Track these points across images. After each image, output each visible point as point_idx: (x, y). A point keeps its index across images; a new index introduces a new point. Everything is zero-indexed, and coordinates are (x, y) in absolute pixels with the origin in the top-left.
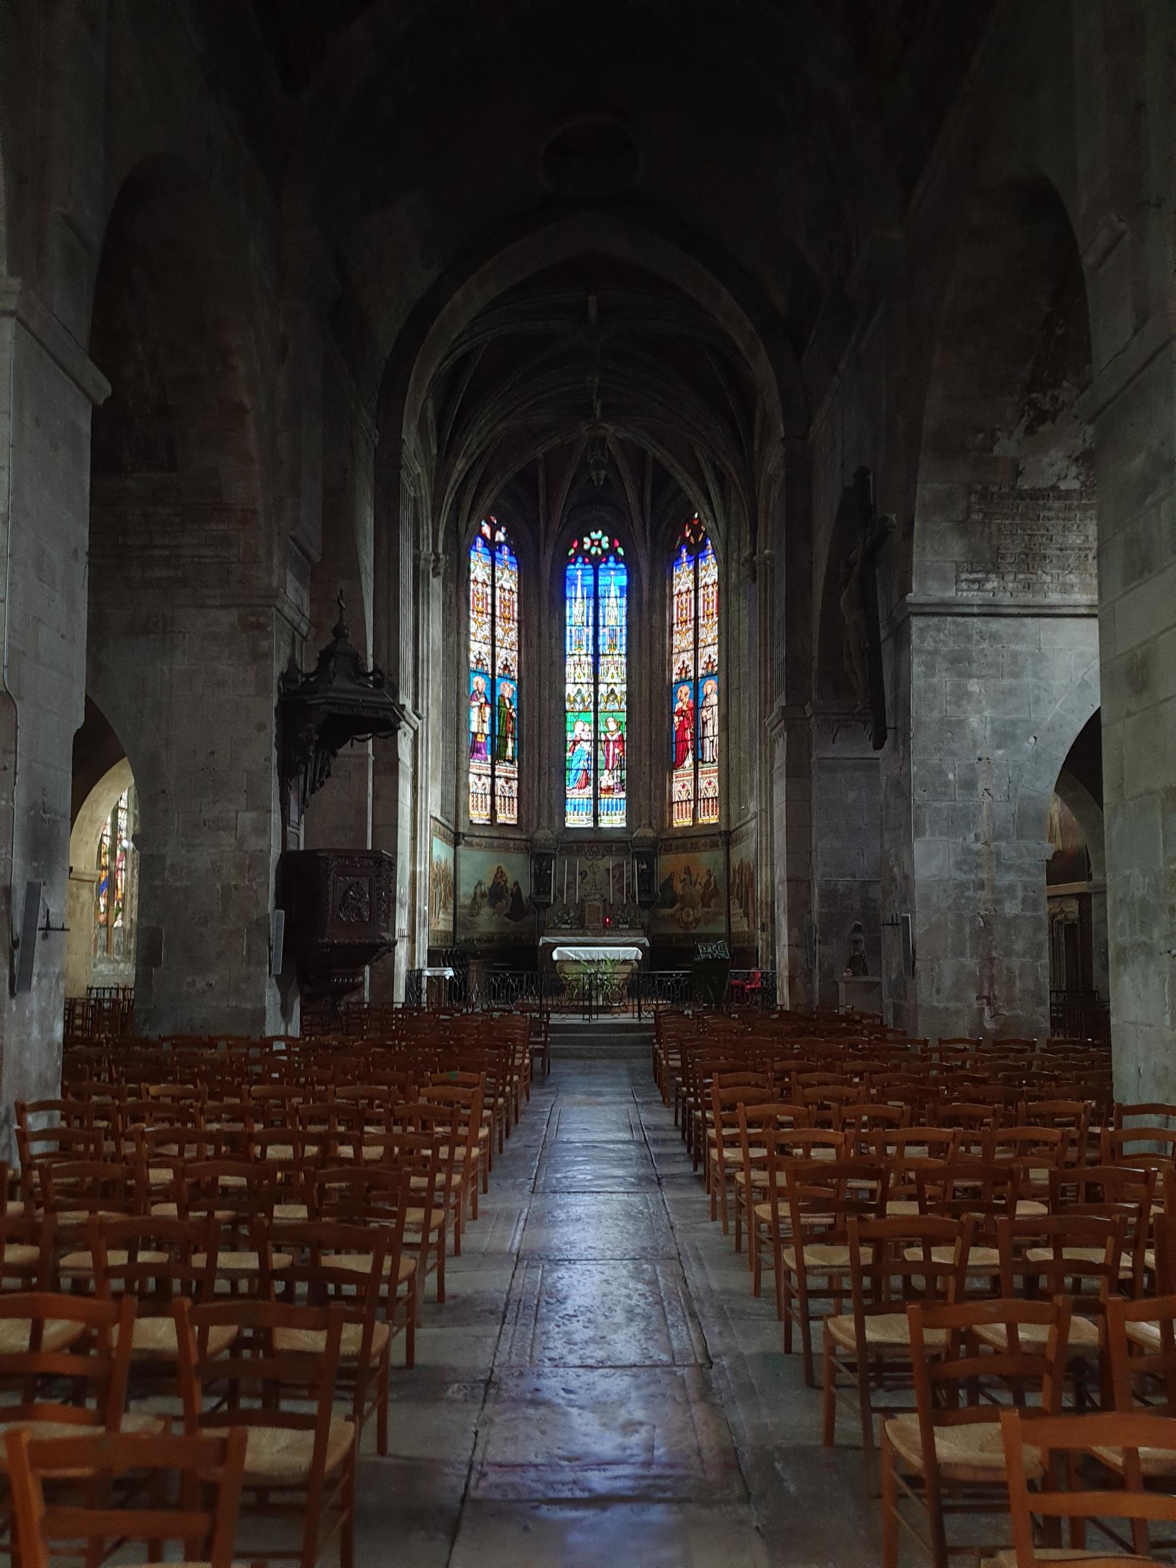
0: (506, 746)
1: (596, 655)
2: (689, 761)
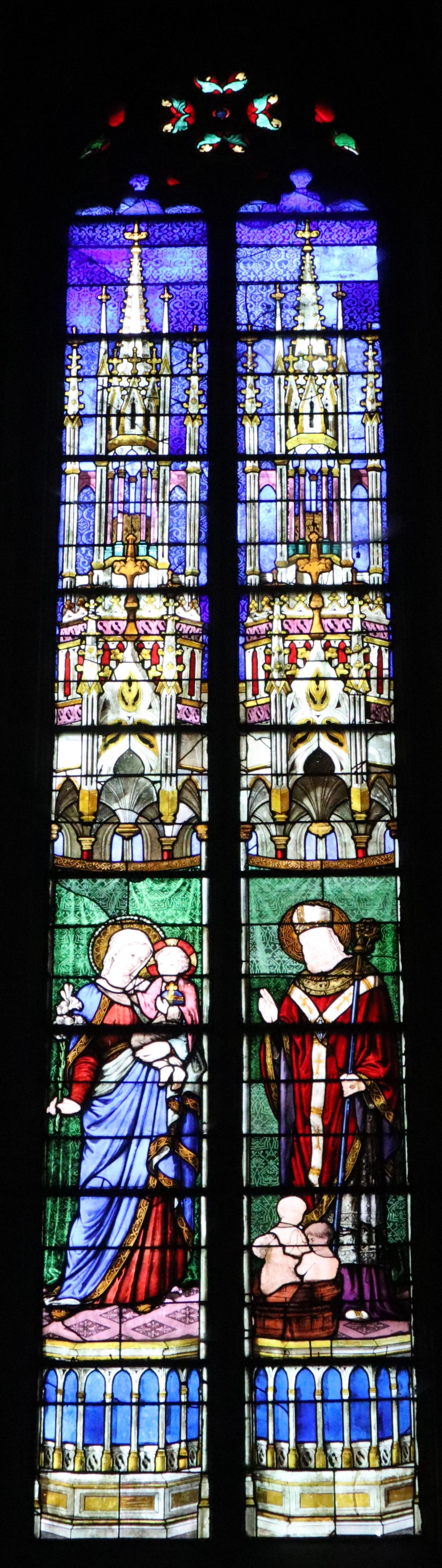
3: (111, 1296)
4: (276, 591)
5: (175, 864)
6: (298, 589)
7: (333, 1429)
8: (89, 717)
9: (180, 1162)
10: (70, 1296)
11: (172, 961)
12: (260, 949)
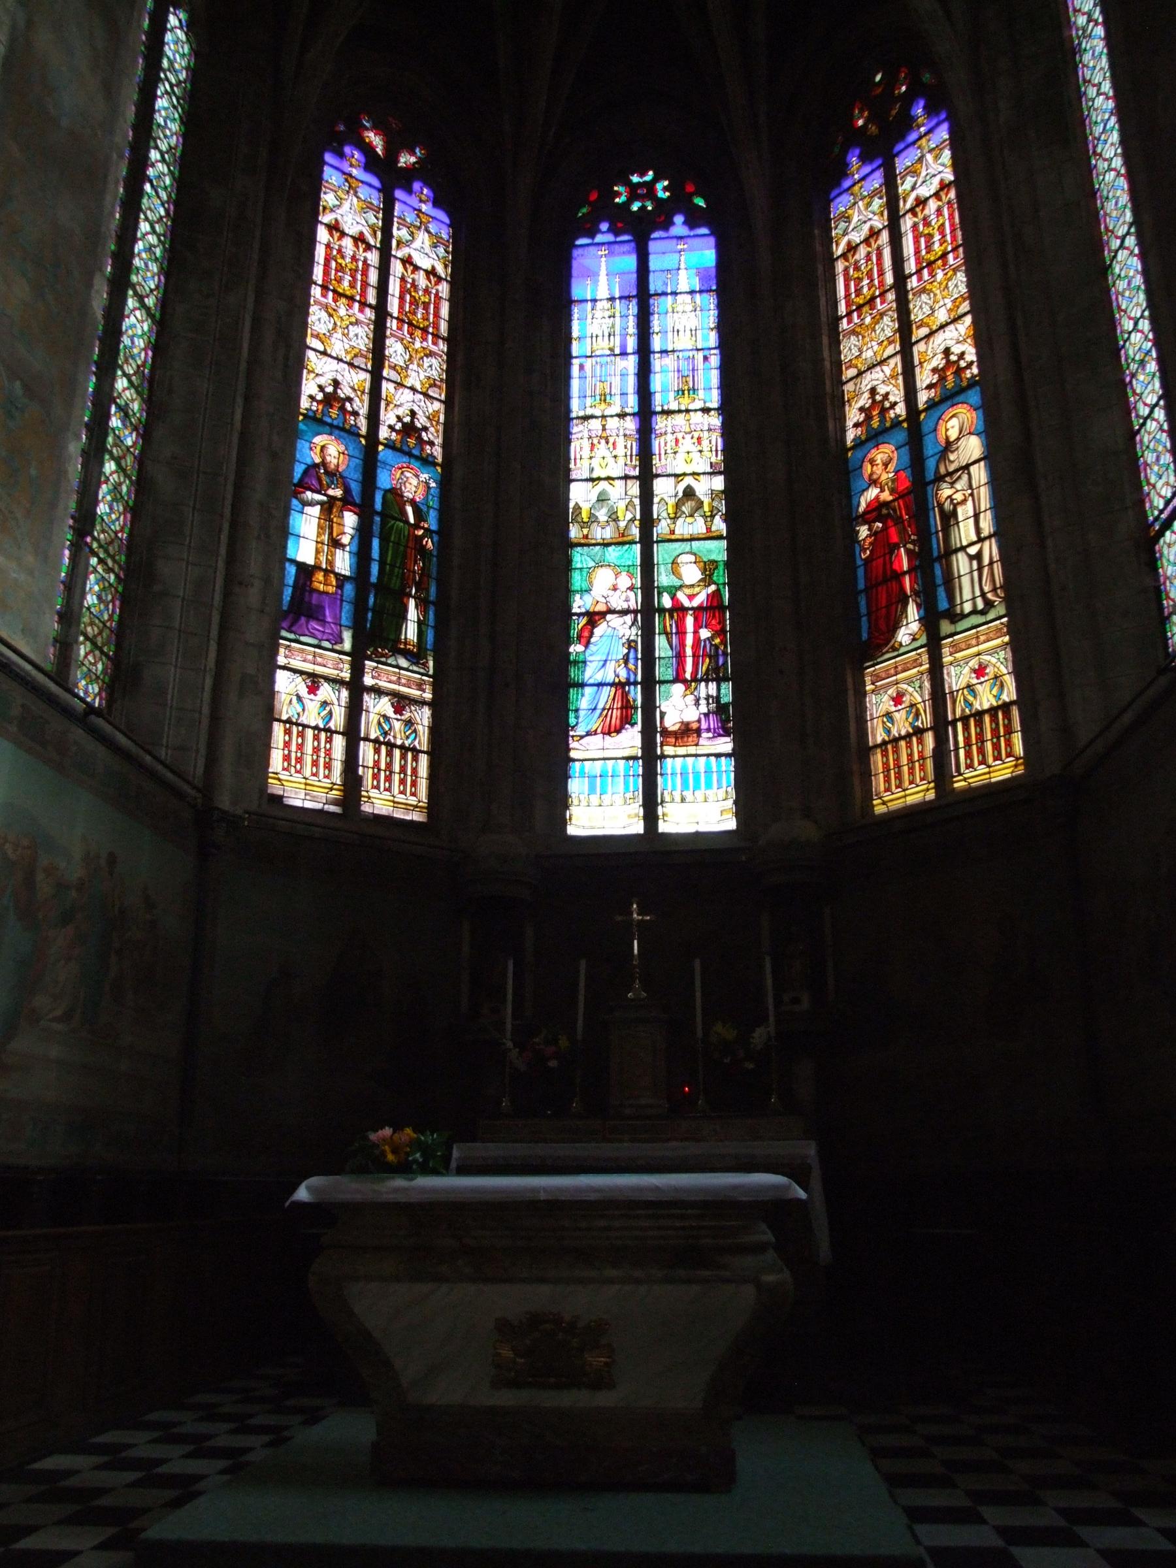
0: (404, 618)
1: (645, 414)
2: (910, 629)
3: (599, 731)
4: (668, 413)
5: (625, 539)
6: (680, 411)
7: (697, 787)
8: (586, 475)
9: (629, 670)
10: (581, 731)
11: (624, 582)
12: (663, 574)
